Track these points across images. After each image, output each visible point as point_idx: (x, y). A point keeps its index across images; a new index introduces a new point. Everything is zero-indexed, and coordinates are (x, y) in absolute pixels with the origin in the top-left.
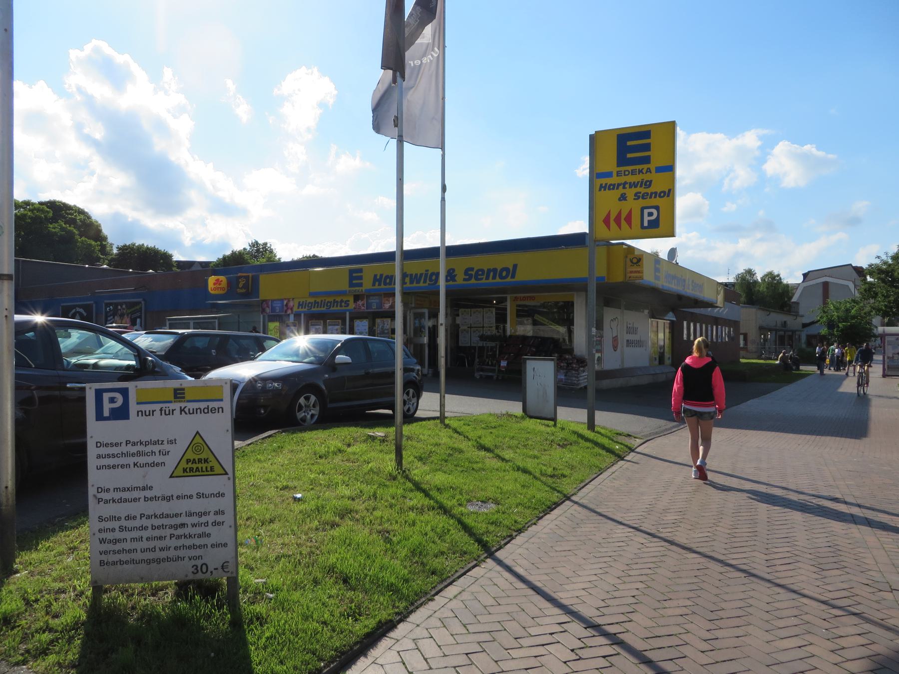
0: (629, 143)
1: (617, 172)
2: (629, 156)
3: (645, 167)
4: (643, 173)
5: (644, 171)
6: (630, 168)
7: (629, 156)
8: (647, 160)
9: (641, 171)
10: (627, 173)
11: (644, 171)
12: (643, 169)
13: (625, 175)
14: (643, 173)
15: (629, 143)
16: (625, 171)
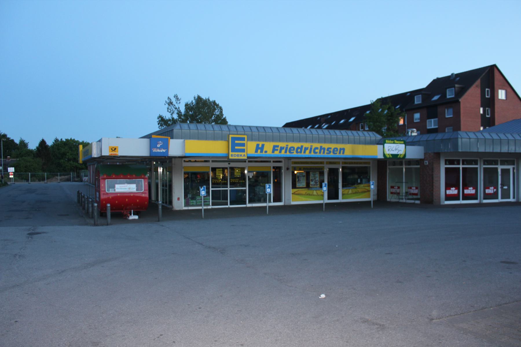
0: (236, 142)
1: (231, 155)
2: (236, 148)
3: (243, 154)
4: (242, 156)
5: (243, 156)
6: (237, 153)
7: (236, 148)
8: (243, 151)
9: (241, 155)
10: (235, 155)
11: (243, 156)
12: (242, 155)
13: (234, 156)
14: (242, 156)
15: (236, 142)
16: (234, 155)
